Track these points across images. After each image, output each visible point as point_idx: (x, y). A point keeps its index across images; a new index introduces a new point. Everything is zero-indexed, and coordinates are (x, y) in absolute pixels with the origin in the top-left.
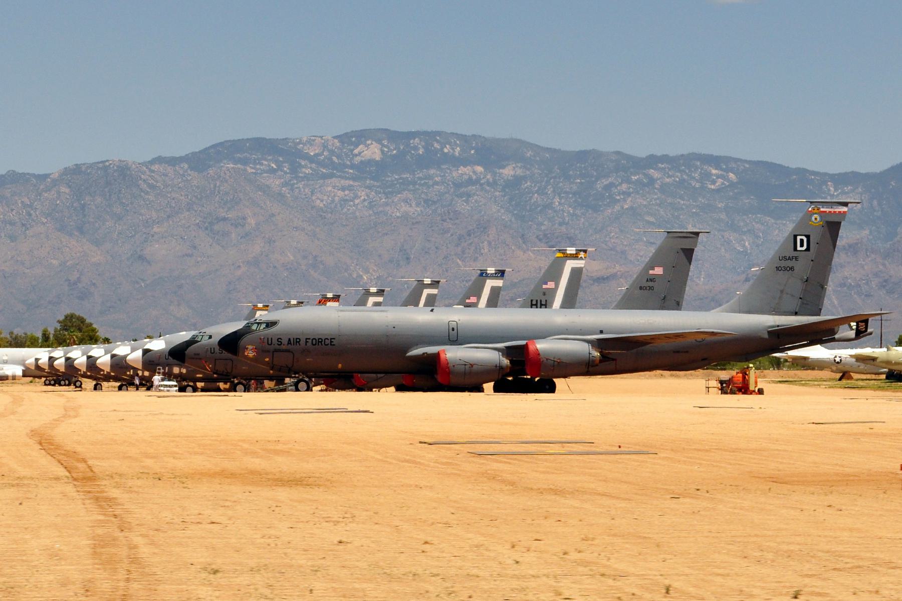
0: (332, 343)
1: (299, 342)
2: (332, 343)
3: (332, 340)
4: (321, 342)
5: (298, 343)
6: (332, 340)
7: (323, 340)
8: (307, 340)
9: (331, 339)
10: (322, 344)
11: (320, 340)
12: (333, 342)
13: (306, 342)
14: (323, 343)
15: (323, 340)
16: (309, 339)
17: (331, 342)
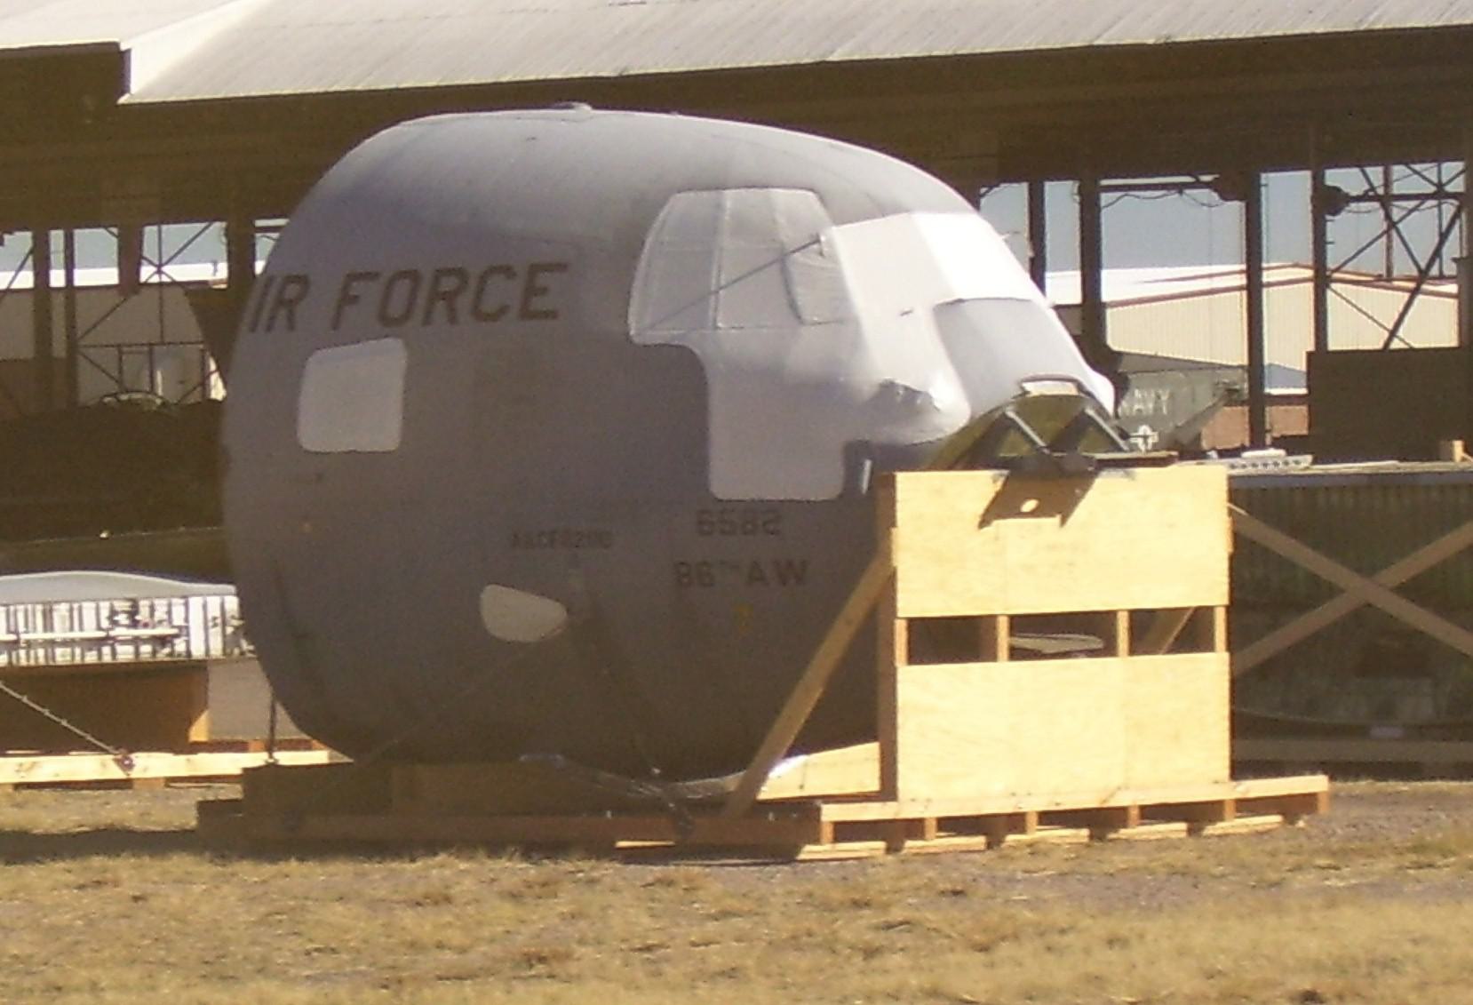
0: (538, 303)
1: (290, 304)
2: (538, 303)
3: (543, 279)
4: (449, 297)
5: (283, 312)
6: (543, 279)
7: (473, 283)
8: (357, 288)
9: (535, 269)
10: (453, 318)
11: (448, 284)
12: (544, 291)
13: (347, 299)
14: (464, 302)
15: (473, 283)
16: (372, 276)
17: (531, 291)
